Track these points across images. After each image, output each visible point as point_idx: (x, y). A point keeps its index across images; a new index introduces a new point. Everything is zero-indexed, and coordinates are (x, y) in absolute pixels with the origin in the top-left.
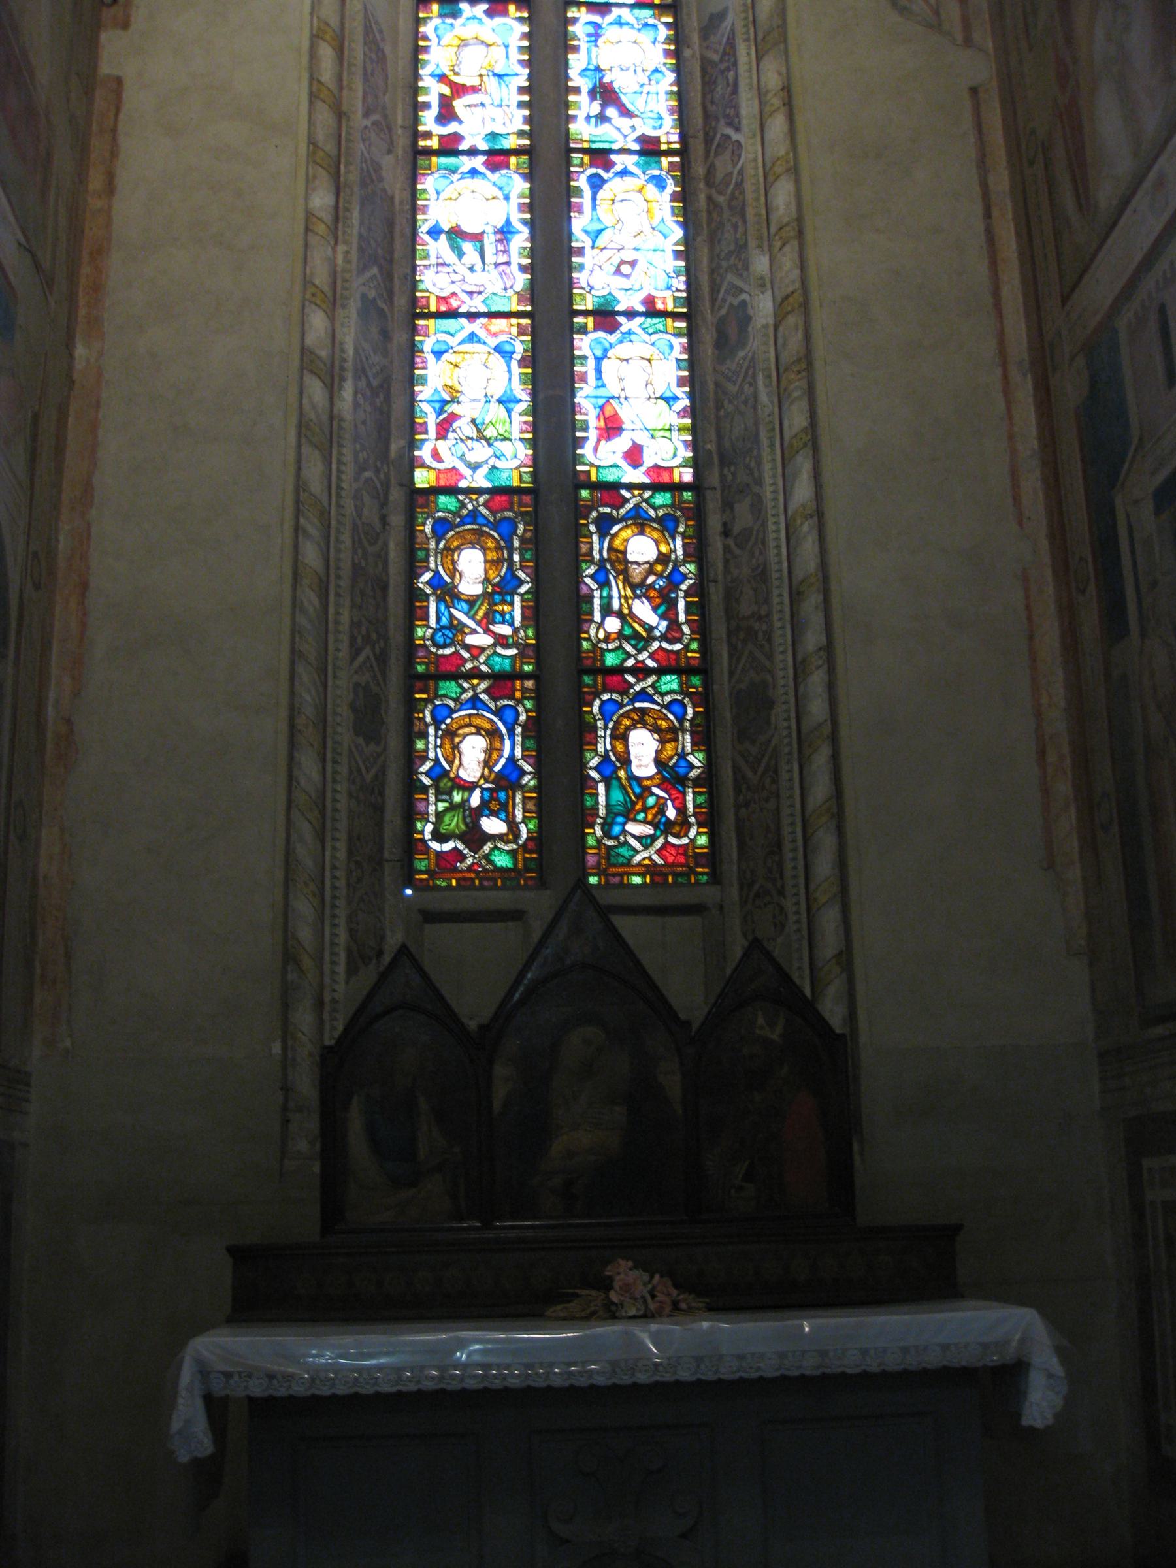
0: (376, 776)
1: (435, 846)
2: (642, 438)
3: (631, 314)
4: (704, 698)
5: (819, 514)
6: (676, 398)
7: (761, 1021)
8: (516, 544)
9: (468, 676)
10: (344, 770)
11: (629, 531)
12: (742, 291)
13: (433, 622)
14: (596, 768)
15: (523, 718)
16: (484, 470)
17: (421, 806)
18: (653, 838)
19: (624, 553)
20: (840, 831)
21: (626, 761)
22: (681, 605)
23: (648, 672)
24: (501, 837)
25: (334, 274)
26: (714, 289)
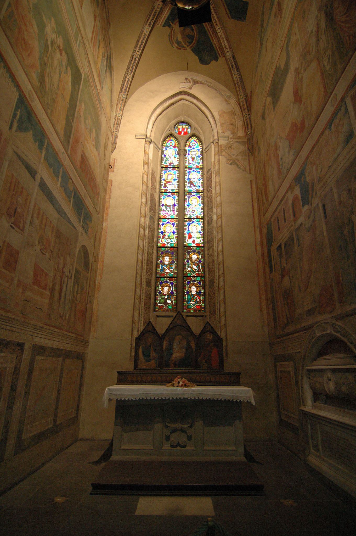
0: (150, 293)
1: (159, 305)
2: (195, 239)
3: (194, 219)
4: (204, 281)
6: (201, 232)
7: (208, 335)
8: (174, 256)
9: (165, 277)
10: (144, 292)
11: (192, 254)
12: (211, 215)
13: (160, 268)
14: (186, 292)
15: (174, 284)
16: (169, 244)
17: (157, 298)
18: (195, 304)
19: (192, 257)
20: (225, 304)
21: (191, 291)
22: (201, 266)
23: (195, 277)
24: (170, 303)
25: (145, 212)
26: (207, 215)
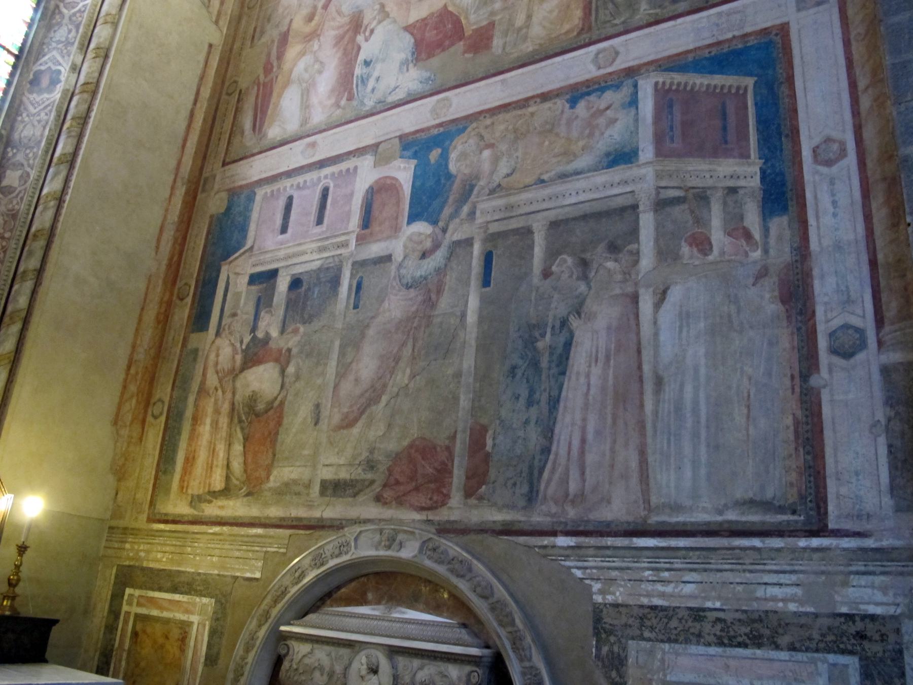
5: (60, 201)
12: (60, 64)
